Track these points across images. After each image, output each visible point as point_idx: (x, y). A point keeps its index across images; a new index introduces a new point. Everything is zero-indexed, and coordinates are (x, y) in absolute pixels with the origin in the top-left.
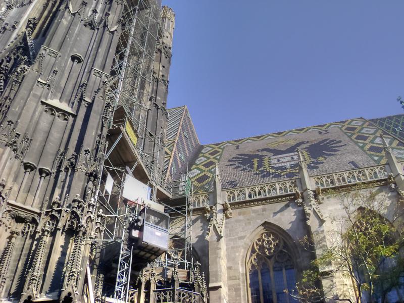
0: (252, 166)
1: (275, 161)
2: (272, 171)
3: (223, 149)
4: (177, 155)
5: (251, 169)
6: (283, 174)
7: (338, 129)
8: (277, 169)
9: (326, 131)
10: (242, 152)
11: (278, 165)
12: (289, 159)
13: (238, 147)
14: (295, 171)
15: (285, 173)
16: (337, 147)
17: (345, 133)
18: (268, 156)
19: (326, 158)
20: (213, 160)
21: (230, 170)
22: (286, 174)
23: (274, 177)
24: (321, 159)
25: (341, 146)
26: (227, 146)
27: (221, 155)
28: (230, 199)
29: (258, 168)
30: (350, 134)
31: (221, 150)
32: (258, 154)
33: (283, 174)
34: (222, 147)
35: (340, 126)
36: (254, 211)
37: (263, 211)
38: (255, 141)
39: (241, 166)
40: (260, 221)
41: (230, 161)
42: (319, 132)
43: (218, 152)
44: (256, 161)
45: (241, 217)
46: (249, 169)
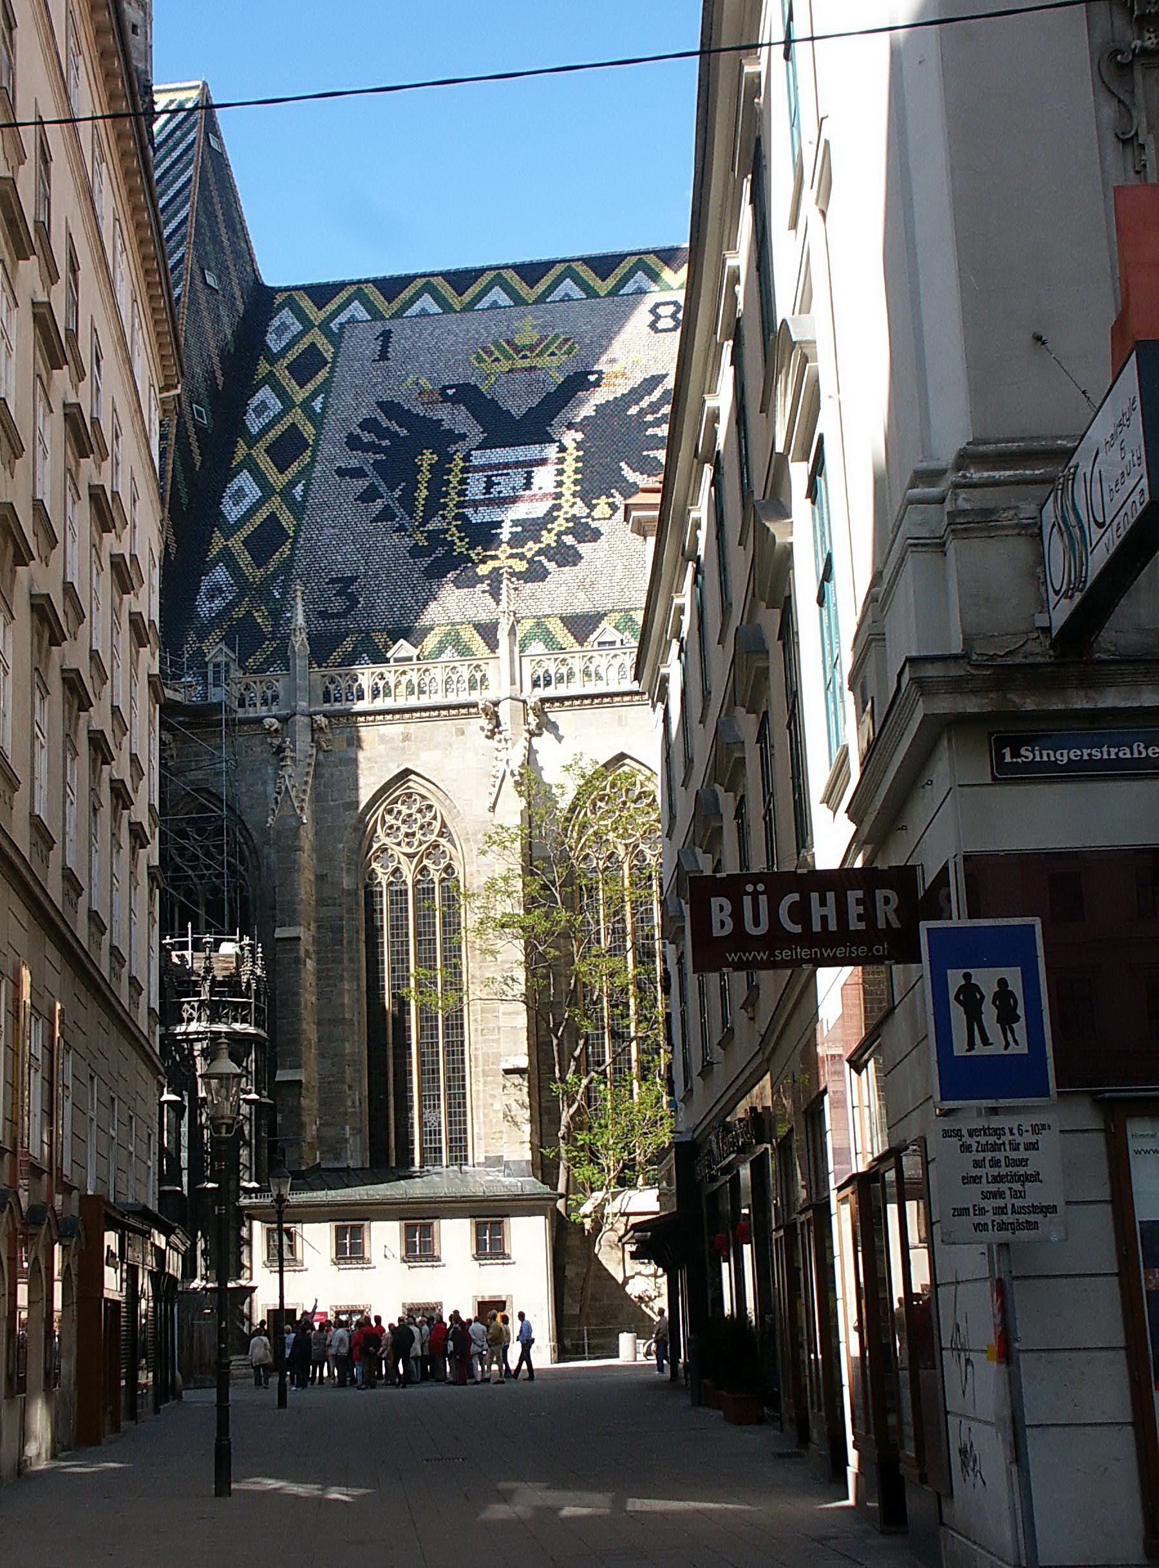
0: (408, 501)
4: (188, 418)
20: (296, 416)
26: (353, 320)
34: (334, 326)
37: (404, 740)
39: (383, 488)
44: (428, 458)
46: (400, 512)
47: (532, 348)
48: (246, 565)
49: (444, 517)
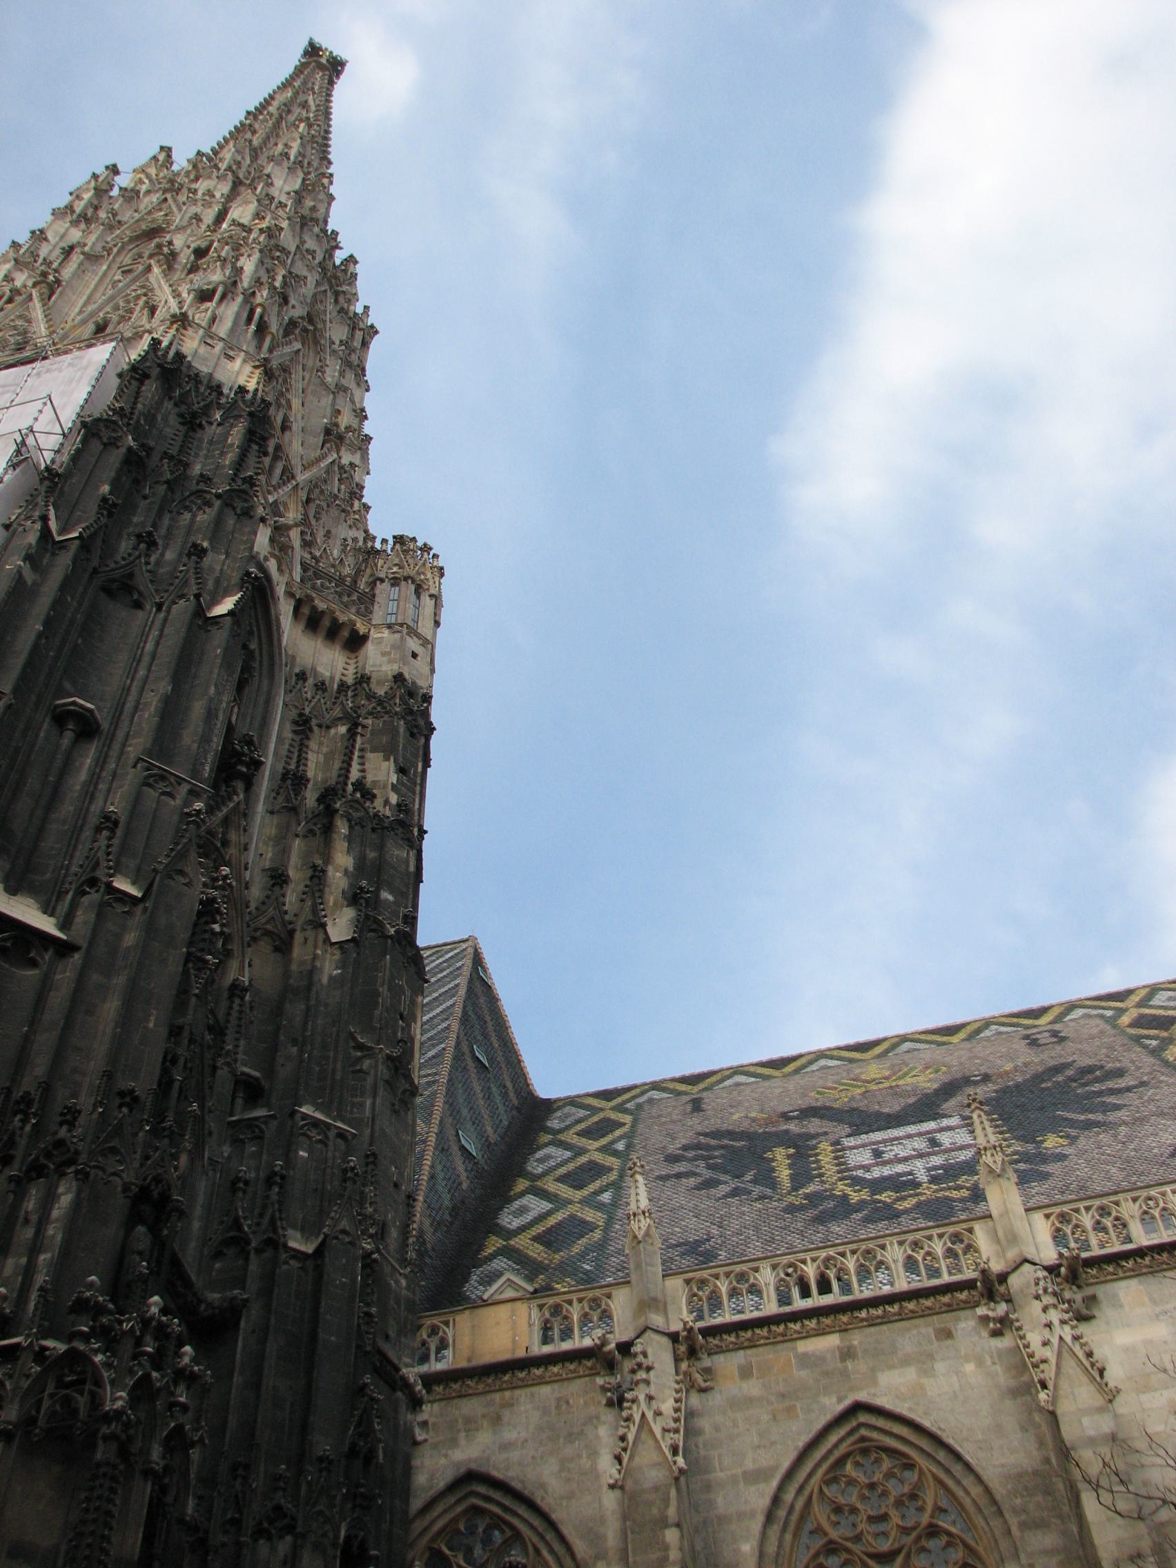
0: (767, 1178)
1: (865, 1157)
2: (855, 1197)
3: (636, 1112)
5: (768, 1192)
6: (907, 1204)
7: (1098, 1021)
8: (877, 1185)
9: (1055, 1034)
10: (714, 1123)
11: (876, 1173)
12: (921, 1144)
13: (697, 1105)
14: (955, 1194)
15: (914, 1201)
16: (1112, 1092)
17: (1137, 1039)
18: (831, 1137)
19: (1073, 1140)
21: (679, 1195)
22: (918, 1205)
23: (867, 1220)
24: (1051, 1142)
25: (1129, 1089)
26: (650, 1101)
27: (629, 1136)
28: (700, 1310)
29: (796, 1187)
30: (1154, 1043)
31: (628, 1119)
32: (787, 1132)
33: (907, 1204)
34: (628, 1106)
35: (1109, 1013)
36: (806, 1360)
38: (767, 1078)
39: (723, 1178)
40: (834, 1400)
41: (672, 1159)
42: (1027, 1037)
43: (612, 1125)
45: (752, 1388)
46: (757, 1190)
47: (887, 1078)
48: (539, 1254)
49: (822, 1182)
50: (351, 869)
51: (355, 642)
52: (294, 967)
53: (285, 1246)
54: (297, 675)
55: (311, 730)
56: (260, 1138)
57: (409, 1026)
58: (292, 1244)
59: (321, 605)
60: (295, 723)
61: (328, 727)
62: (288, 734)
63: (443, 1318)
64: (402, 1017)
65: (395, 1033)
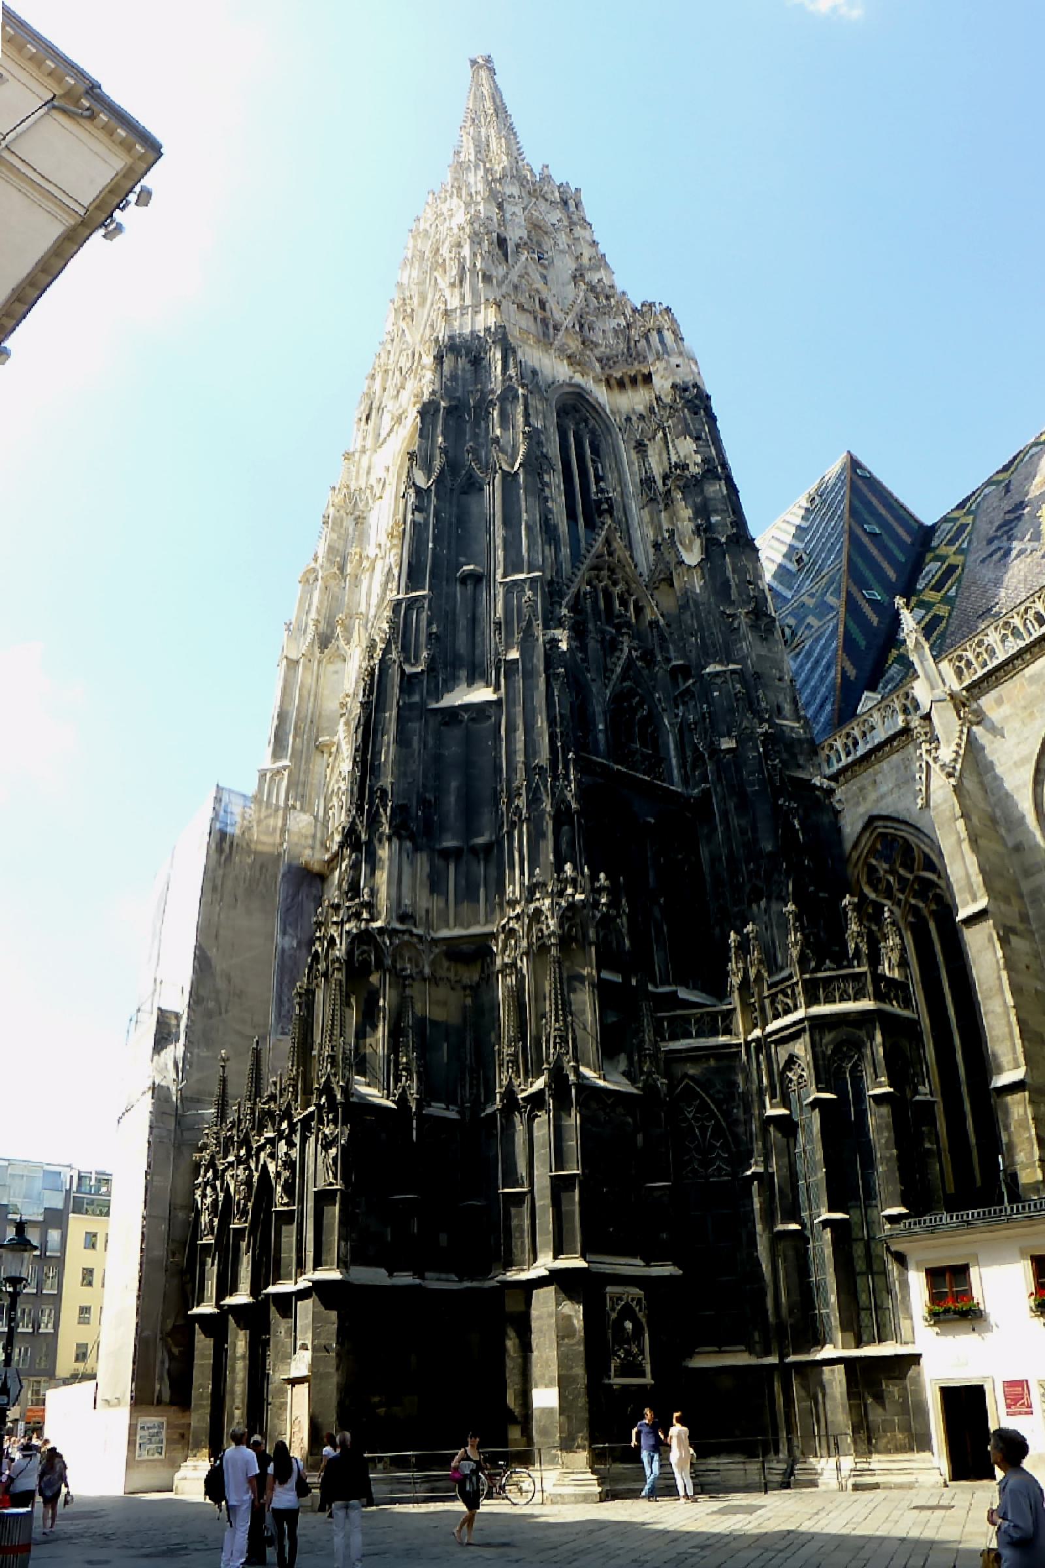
50: (691, 516)
51: (648, 379)
52: (678, 594)
53: (720, 749)
54: (626, 420)
55: (645, 446)
56: (692, 697)
57: (757, 585)
58: (723, 747)
59: (618, 375)
60: (635, 448)
61: (654, 438)
62: (634, 456)
63: (850, 726)
64: (750, 583)
65: (748, 595)
